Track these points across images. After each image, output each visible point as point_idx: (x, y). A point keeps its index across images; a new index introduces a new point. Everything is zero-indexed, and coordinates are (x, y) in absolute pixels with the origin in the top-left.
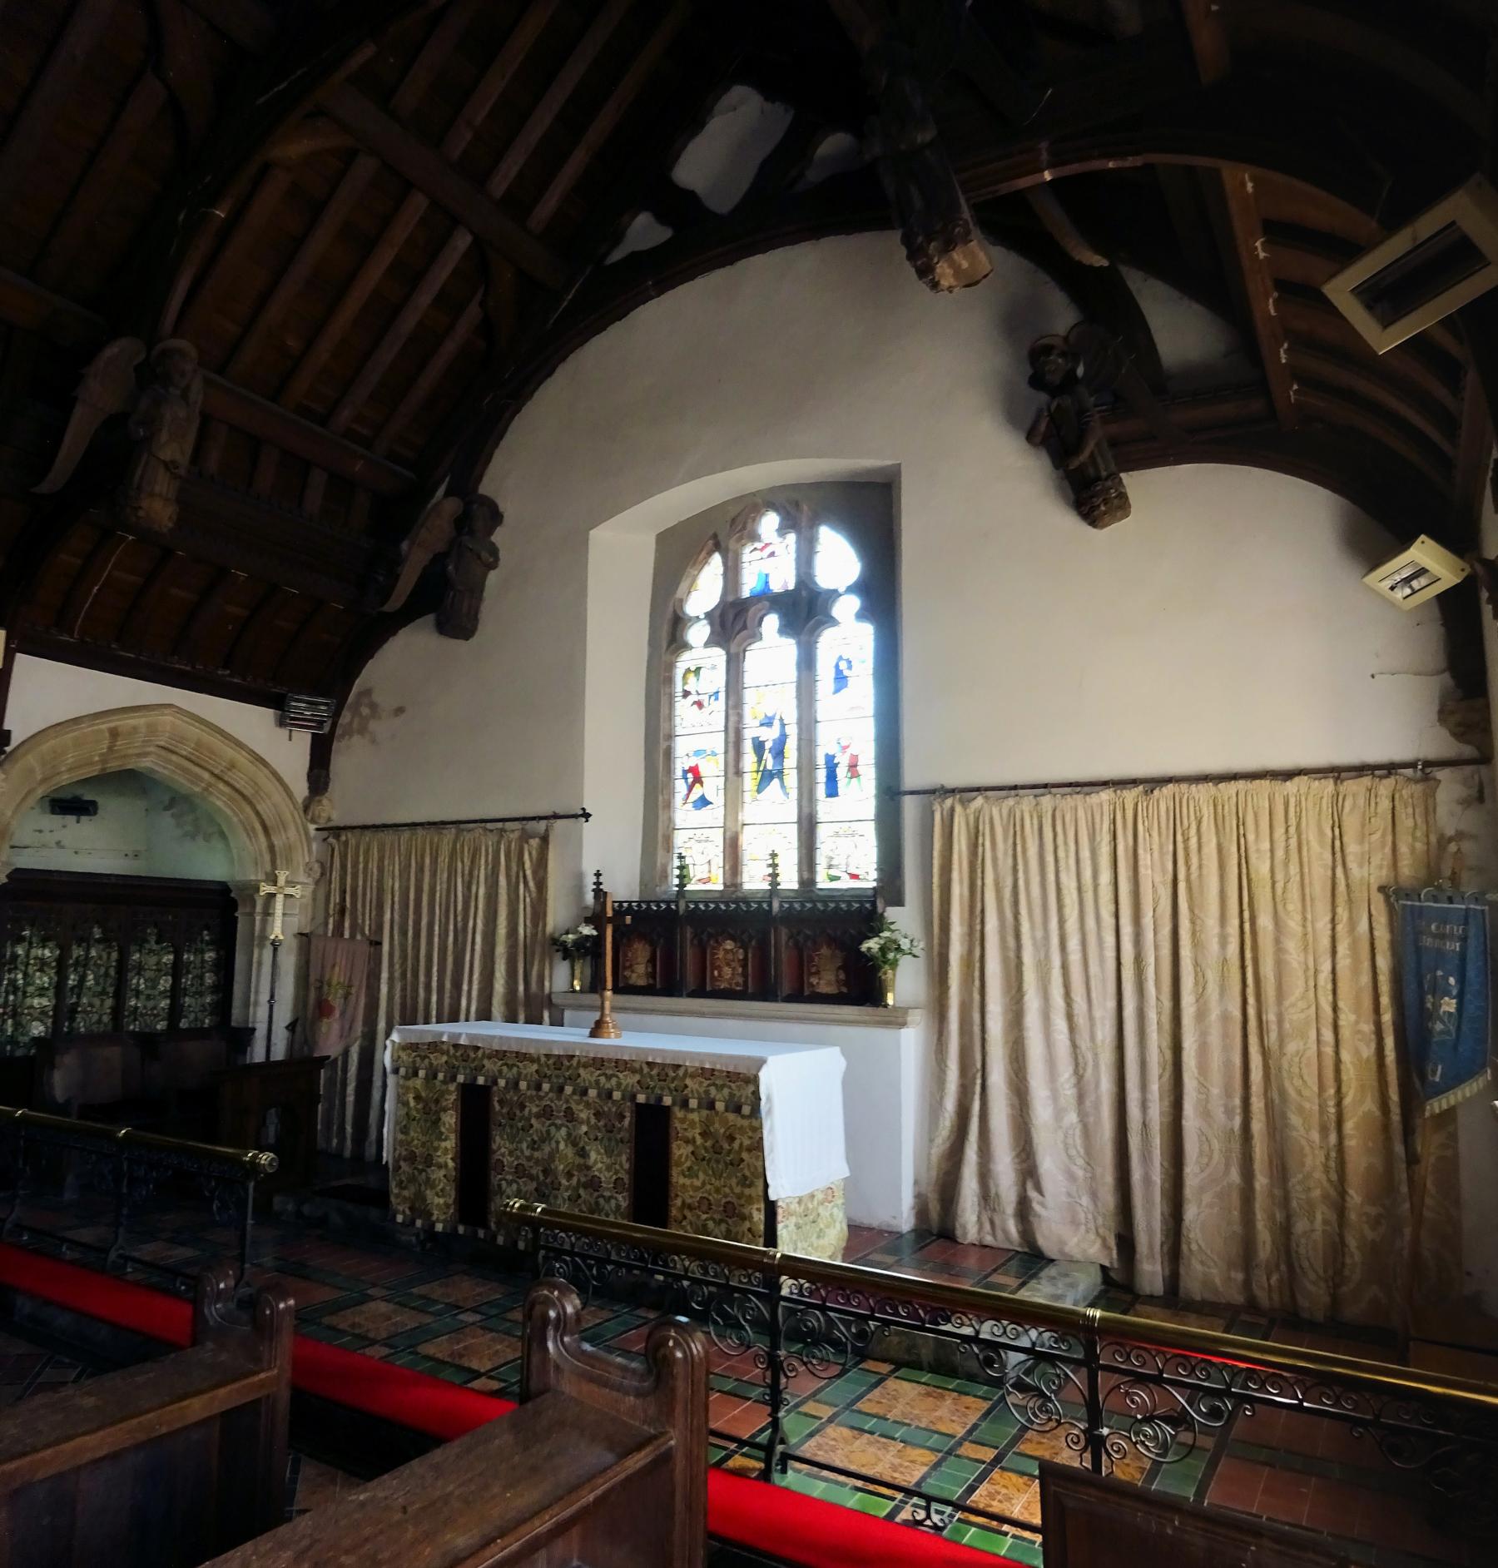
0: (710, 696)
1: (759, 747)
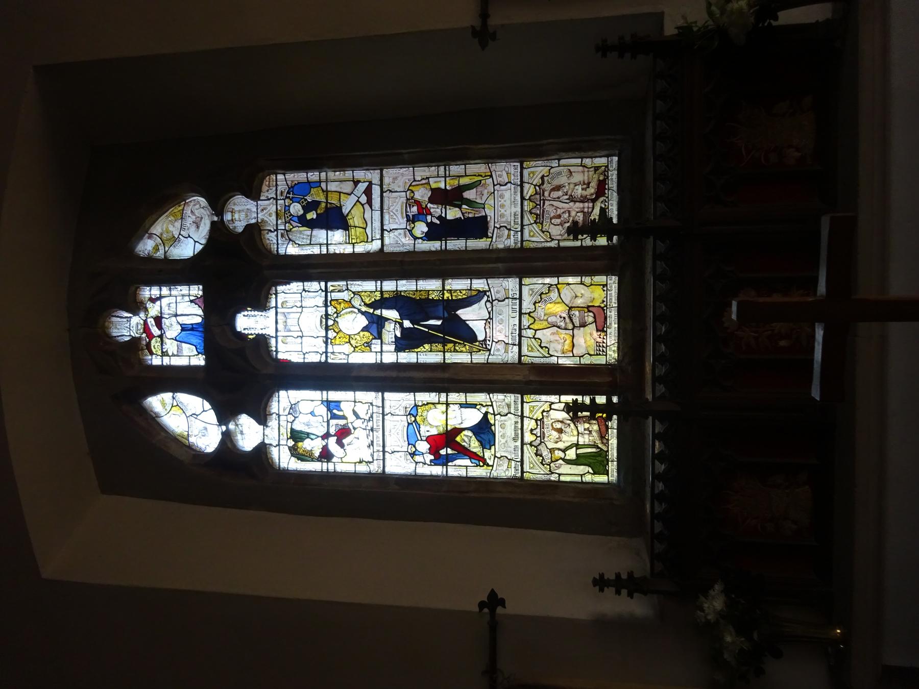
0: (334, 417)
1: (406, 341)
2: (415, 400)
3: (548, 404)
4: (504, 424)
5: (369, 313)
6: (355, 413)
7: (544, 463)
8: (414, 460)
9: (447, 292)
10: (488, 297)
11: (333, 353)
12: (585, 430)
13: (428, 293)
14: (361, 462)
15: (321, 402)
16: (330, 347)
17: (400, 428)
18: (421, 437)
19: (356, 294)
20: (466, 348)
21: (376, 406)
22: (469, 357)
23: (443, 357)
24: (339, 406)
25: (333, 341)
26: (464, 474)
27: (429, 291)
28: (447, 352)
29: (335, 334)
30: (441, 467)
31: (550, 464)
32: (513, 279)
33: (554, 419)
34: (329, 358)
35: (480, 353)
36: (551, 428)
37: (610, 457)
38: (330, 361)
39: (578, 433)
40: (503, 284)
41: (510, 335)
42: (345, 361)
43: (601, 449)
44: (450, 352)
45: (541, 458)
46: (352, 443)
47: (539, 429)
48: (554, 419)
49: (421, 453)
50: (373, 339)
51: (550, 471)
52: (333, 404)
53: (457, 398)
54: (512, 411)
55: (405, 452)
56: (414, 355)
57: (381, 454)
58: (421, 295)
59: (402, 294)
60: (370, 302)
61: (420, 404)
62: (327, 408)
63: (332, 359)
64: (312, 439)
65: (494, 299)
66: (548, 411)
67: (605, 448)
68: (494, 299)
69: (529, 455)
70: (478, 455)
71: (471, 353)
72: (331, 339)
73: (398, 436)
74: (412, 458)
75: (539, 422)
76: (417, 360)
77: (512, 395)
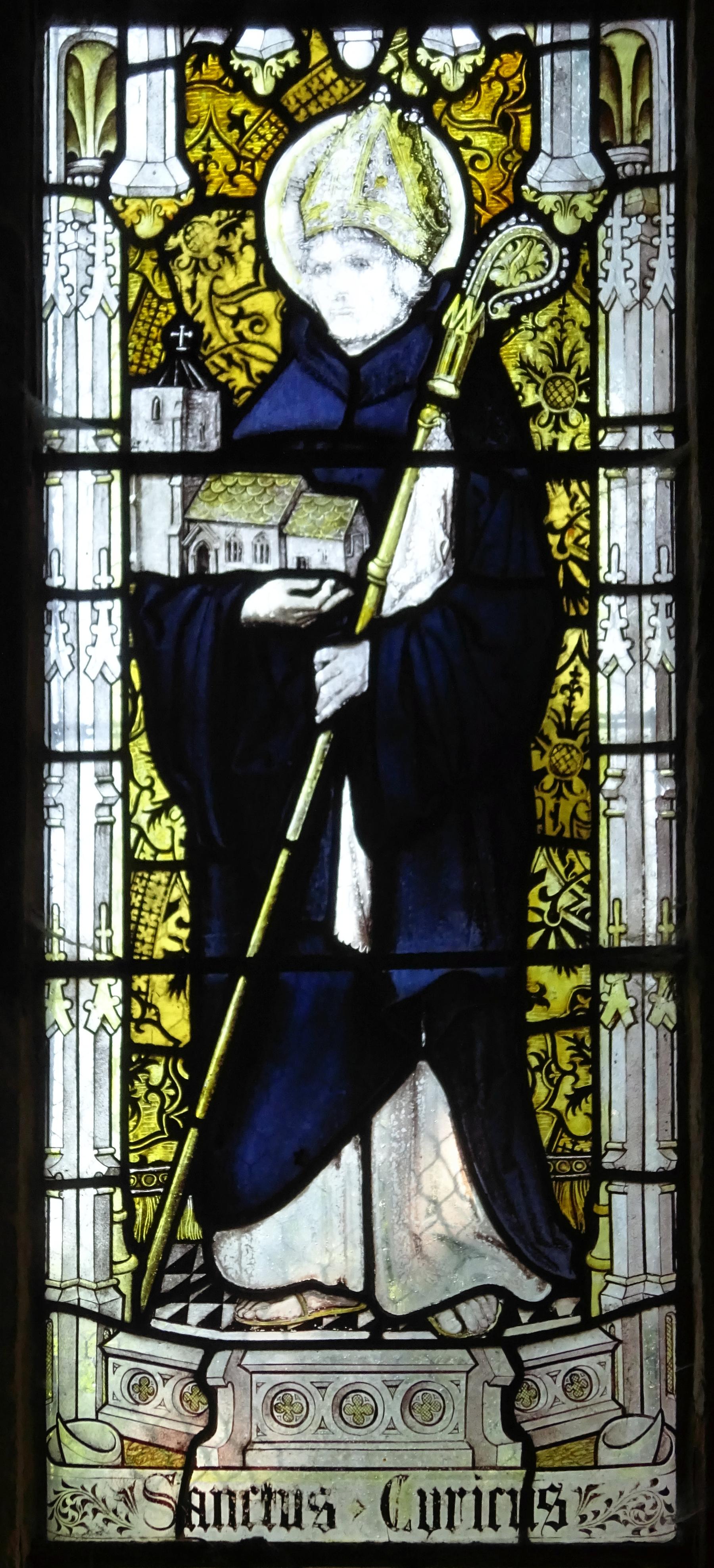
5: (429, 369)
9: (581, 991)
10: (543, 1310)
13: (577, 844)
19: (574, 258)
20: (152, 1140)
22: (92, 1167)
23: (87, 955)
25: (212, 67)
27: (592, 847)
28: (129, 994)
29: (263, 85)
32: (671, 1499)
35: (119, 1253)
40: (634, 1425)
41: (260, 1478)
44: (126, 1019)
50: (227, 393)
58: (563, 781)
59: (572, 638)
60: (515, 376)
63: (70, 61)
65: (527, 1354)
68: (527, 1354)
72: (224, 53)
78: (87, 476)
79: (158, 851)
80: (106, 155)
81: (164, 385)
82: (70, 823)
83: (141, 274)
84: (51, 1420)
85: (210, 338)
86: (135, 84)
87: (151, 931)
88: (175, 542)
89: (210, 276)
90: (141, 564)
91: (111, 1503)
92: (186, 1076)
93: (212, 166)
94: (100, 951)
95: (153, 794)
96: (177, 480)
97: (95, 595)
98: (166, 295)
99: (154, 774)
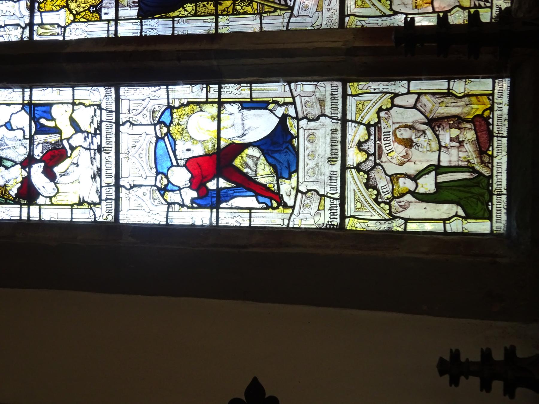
0: (42, 130)
2: (168, 99)
3: (389, 96)
4: (313, 134)
6: (73, 123)
7: (380, 200)
8: (165, 200)
11: (41, 25)
12: (451, 140)
14: (81, 203)
15: (21, 106)
16: (37, 16)
17: (145, 146)
18: (176, 160)
20: (253, 8)
21: (106, 110)
23: (214, 24)
24: (50, 113)
25: (42, 5)
26: (246, 223)
30: (209, 210)
31: (391, 201)
33: (397, 123)
34: (35, 33)
35: (276, 14)
36: (392, 138)
37: (495, 186)
38: (36, 38)
39: (440, 146)
42: (60, 38)
43: (480, 174)
44: (227, 15)
45: (375, 192)
46: (68, 171)
47: (373, 141)
48: (397, 123)
49: (177, 188)
51: (390, 214)
52: (39, 108)
53: (236, 92)
54: (328, 111)
55: (152, 186)
56: (169, 22)
57: (113, 190)
61: (177, 104)
62: (30, 114)
63: (40, 35)
64: (7, 168)
66: (388, 109)
67: (487, 173)
69: (355, 187)
70: (269, 189)
71: (261, 15)
72: (40, 3)
73: (140, 160)
74: (163, 196)
75: (372, 130)
76: (173, 30)
77: (328, 84)
78: (119, 28)
79: (193, 9)
80: (58, 27)
81: (101, 12)
82: (187, 29)
83: (80, 18)
84: (312, 28)
85: (93, 3)
86: (45, 22)
87: (209, 10)
88: (132, 8)
89: (81, 4)
90: (136, 16)
91: (330, 13)
92: (239, 1)
93: (60, 5)
94: (213, 21)
95: (181, 11)
96: (120, 9)
97: (142, 26)
98: (84, 13)
99: (177, 11)
